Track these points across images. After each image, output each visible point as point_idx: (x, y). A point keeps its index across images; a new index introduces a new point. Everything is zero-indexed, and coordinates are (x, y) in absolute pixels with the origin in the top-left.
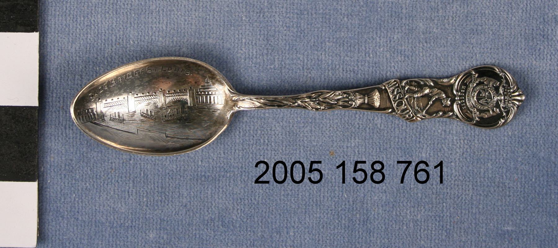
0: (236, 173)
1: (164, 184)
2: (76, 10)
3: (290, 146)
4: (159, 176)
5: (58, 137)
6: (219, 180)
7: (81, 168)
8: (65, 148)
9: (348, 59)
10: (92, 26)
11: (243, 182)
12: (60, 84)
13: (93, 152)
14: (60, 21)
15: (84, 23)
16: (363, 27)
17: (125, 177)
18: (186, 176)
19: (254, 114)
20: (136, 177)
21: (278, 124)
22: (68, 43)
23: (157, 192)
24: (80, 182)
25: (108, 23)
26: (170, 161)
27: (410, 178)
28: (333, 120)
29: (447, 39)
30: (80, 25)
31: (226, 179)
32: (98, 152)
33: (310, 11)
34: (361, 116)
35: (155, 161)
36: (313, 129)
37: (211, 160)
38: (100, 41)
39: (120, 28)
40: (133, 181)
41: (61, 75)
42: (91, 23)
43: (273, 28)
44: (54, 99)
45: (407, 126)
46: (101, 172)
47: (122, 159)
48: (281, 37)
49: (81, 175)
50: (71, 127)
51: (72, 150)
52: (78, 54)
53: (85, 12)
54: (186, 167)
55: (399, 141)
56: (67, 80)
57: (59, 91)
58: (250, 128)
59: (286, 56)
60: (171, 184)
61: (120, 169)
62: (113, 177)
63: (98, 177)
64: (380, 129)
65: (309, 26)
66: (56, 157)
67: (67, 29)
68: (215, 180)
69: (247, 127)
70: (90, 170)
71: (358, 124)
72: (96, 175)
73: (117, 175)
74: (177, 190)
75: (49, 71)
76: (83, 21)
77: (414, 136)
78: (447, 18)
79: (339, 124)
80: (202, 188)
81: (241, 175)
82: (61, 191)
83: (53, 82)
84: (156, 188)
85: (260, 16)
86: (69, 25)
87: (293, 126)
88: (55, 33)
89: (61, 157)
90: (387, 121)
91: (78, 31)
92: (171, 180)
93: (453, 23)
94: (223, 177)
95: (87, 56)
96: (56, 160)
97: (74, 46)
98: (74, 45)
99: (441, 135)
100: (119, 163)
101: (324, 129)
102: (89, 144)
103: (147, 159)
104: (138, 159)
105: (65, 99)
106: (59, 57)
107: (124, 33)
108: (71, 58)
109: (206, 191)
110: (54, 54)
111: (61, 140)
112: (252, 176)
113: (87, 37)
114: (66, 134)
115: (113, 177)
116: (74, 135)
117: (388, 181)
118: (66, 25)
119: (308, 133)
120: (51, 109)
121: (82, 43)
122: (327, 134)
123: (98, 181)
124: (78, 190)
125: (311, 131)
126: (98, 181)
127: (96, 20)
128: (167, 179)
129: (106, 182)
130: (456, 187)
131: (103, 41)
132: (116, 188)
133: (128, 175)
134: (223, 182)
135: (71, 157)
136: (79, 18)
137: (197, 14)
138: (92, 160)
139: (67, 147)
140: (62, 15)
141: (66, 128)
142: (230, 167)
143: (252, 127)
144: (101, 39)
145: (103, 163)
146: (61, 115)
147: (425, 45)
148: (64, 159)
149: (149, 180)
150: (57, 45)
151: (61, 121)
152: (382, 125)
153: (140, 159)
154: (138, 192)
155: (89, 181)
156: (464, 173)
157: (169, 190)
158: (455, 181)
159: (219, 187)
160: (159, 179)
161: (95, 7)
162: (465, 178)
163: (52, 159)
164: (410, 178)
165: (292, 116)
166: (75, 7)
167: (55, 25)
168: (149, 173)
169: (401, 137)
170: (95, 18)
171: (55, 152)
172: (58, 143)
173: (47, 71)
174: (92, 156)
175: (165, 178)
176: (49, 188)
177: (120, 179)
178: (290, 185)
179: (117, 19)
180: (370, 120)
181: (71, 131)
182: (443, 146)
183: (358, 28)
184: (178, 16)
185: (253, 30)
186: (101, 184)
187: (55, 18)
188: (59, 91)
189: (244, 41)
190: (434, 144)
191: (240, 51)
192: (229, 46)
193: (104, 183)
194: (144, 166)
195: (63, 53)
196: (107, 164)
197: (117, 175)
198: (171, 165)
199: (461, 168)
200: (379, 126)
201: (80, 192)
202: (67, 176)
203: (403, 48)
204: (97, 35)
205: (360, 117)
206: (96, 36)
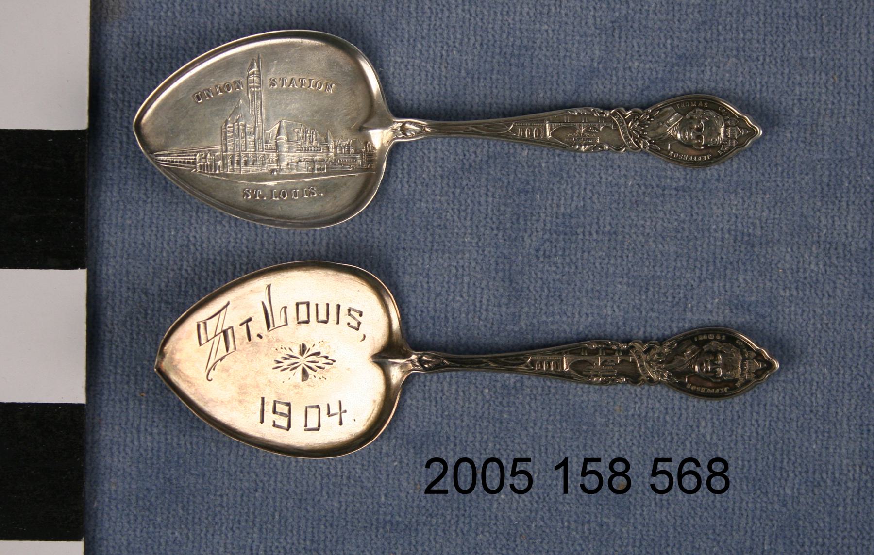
0: (448, 517)
1: (316, 535)
2: (162, 217)
3: (546, 472)
4: (307, 519)
5: (125, 446)
6: (416, 530)
7: (166, 505)
8: (137, 467)
9: (654, 315)
10: (192, 247)
11: (460, 534)
12: (130, 351)
13: (188, 476)
14: (133, 236)
15: (176, 241)
16: (684, 259)
17: (247, 521)
18: (356, 521)
19: (483, 413)
20: (266, 522)
21: (526, 432)
22: (146, 277)
23: (305, 548)
24: (164, 529)
25: (219, 241)
26: (328, 493)
27: (762, 534)
28: (626, 426)
29: (834, 283)
30: (168, 244)
31: (430, 530)
32: (198, 475)
33: (588, 227)
34: (675, 419)
35: (301, 494)
36: (590, 443)
37: (403, 495)
38: (204, 274)
39: (242, 252)
40: (260, 530)
41: (131, 334)
42: (189, 241)
43: (520, 258)
44: (118, 377)
45: (758, 440)
46: (201, 511)
47: (241, 488)
48: (534, 276)
49: (165, 517)
50: (149, 430)
51: (150, 471)
52: (165, 298)
53: (179, 221)
54: (358, 505)
55: (743, 466)
56: (144, 343)
57: (127, 364)
58: (475, 437)
59: (541, 309)
60: (329, 536)
61: (236, 507)
62: (224, 521)
63: (196, 520)
64: (710, 444)
65: (586, 254)
66: (120, 484)
67: (144, 252)
68: (410, 529)
69: (470, 435)
70: (183, 509)
71: (671, 434)
72: (193, 518)
73: (231, 517)
74: (340, 547)
75: (110, 326)
76: (175, 236)
77: (770, 457)
78: (834, 245)
79: (635, 433)
80: (386, 543)
81: (457, 521)
82: (129, 544)
83: (117, 346)
84: (302, 542)
85: (497, 235)
86: (149, 244)
87: (553, 437)
88: (122, 257)
89: (130, 484)
90: (723, 429)
91: (165, 254)
92: (329, 529)
93: (845, 256)
94: (425, 524)
95: (181, 301)
96: (120, 489)
97: (157, 280)
98: (157, 280)
99: (820, 455)
100: (235, 496)
101: (609, 443)
102: (181, 462)
103: (287, 491)
104: (271, 489)
105: (139, 378)
106: (130, 302)
107: (249, 260)
108: (150, 304)
109: (394, 550)
110: (121, 296)
111: (130, 453)
112: (477, 524)
113: (182, 265)
114: (140, 441)
115: (224, 521)
116: (155, 444)
117: (724, 537)
118: (143, 244)
119: (579, 450)
120: (113, 397)
121: (171, 276)
122: (614, 451)
123: (197, 527)
124: (160, 544)
125: (585, 446)
126: (197, 527)
127: (198, 236)
128: (323, 527)
129: (211, 530)
130: (845, 548)
131: (211, 274)
132: (228, 541)
133: (251, 517)
134: (423, 534)
135: (148, 485)
136: (166, 230)
137: (382, 230)
138: (187, 491)
139: (141, 466)
140: (136, 227)
141: (139, 432)
142: (437, 507)
143: (478, 436)
144: (207, 271)
145: (205, 495)
146: (131, 406)
147: (795, 293)
148: (134, 486)
149: (290, 528)
150: (125, 279)
151: (130, 418)
152: (715, 437)
153: (274, 490)
154: (268, 550)
155: (181, 528)
156: (860, 526)
157: (326, 546)
158: (843, 539)
159: (417, 543)
160: (306, 527)
161: (197, 212)
162: (862, 533)
163: (113, 488)
164: (762, 534)
165: (552, 418)
166: (160, 212)
167: (123, 242)
168: (289, 514)
169: (748, 458)
170: (196, 232)
171: (119, 473)
172: (124, 458)
173: (107, 326)
174: (187, 484)
175: (318, 524)
176: (107, 540)
177: (236, 525)
178: (545, 542)
179: (236, 234)
180: (691, 427)
181: (149, 438)
182: (824, 476)
183: (675, 260)
184: (348, 232)
185: (482, 260)
186: (202, 535)
187: (124, 230)
188: (127, 364)
189: (466, 279)
190: (807, 472)
191: (458, 298)
192: (439, 289)
193: (207, 531)
194: (281, 502)
195: (136, 294)
196: (212, 497)
197: (231, 517)
198: (329, 501)
199: (856, 516)
200: (708, 437)
201: (162, 547)
202: (140, 518)
203: (753, 298)
204: (200, 263)
205: (674, 421)
206: (197, 264)
